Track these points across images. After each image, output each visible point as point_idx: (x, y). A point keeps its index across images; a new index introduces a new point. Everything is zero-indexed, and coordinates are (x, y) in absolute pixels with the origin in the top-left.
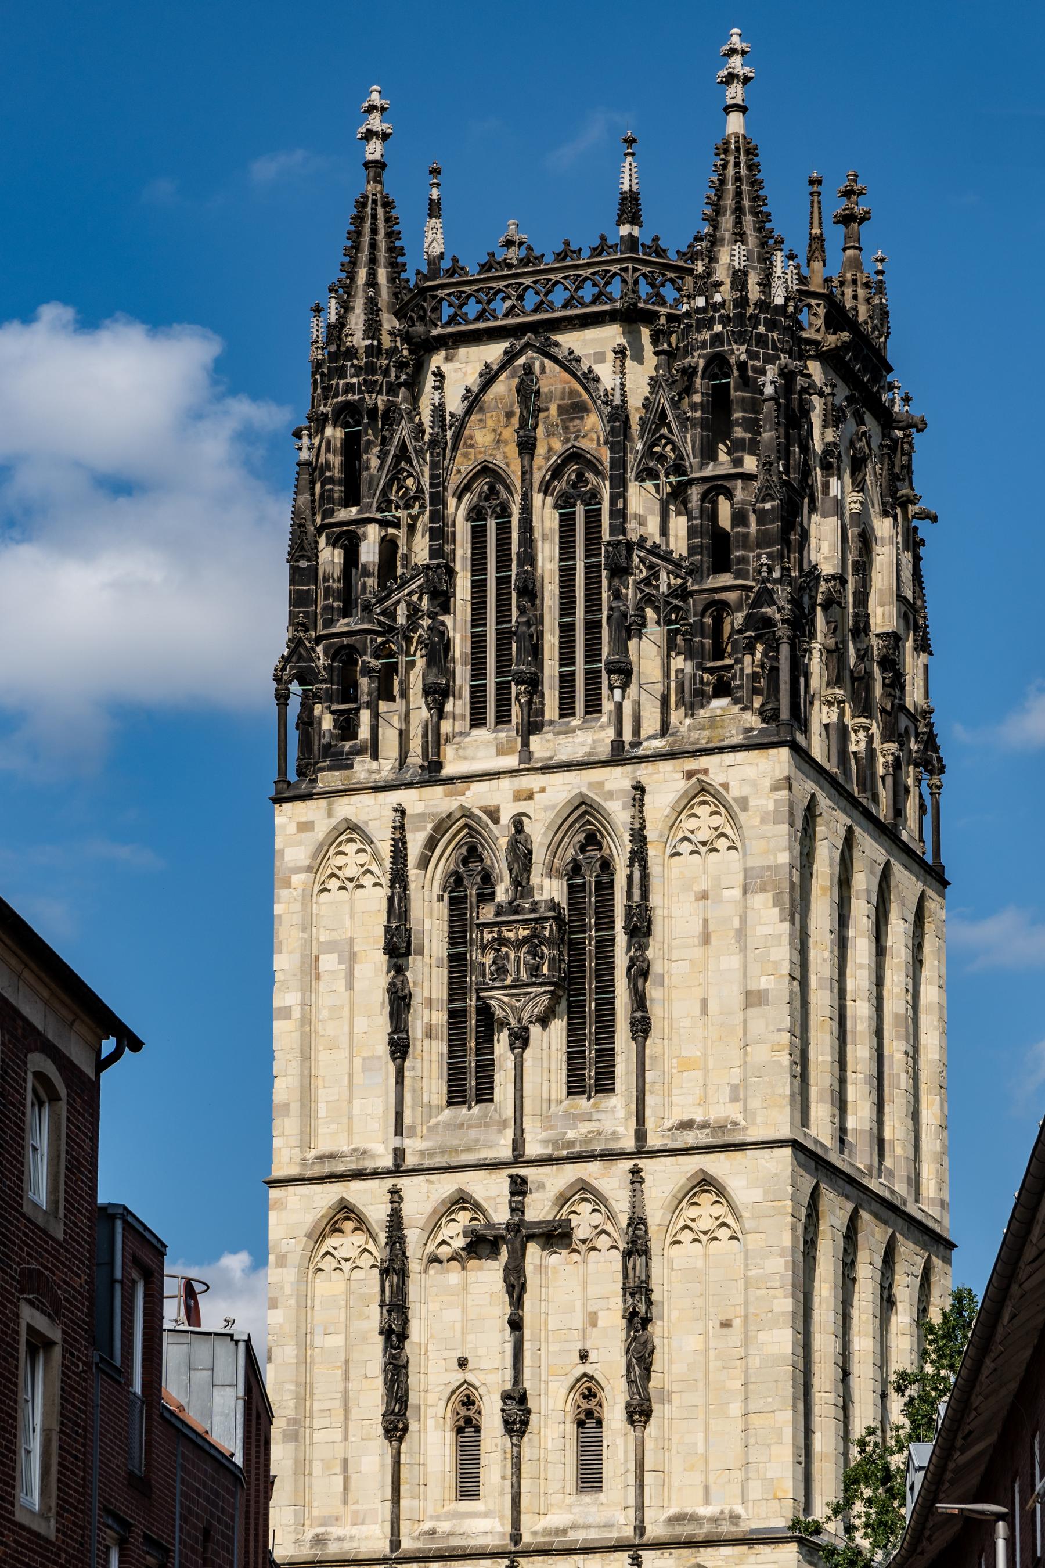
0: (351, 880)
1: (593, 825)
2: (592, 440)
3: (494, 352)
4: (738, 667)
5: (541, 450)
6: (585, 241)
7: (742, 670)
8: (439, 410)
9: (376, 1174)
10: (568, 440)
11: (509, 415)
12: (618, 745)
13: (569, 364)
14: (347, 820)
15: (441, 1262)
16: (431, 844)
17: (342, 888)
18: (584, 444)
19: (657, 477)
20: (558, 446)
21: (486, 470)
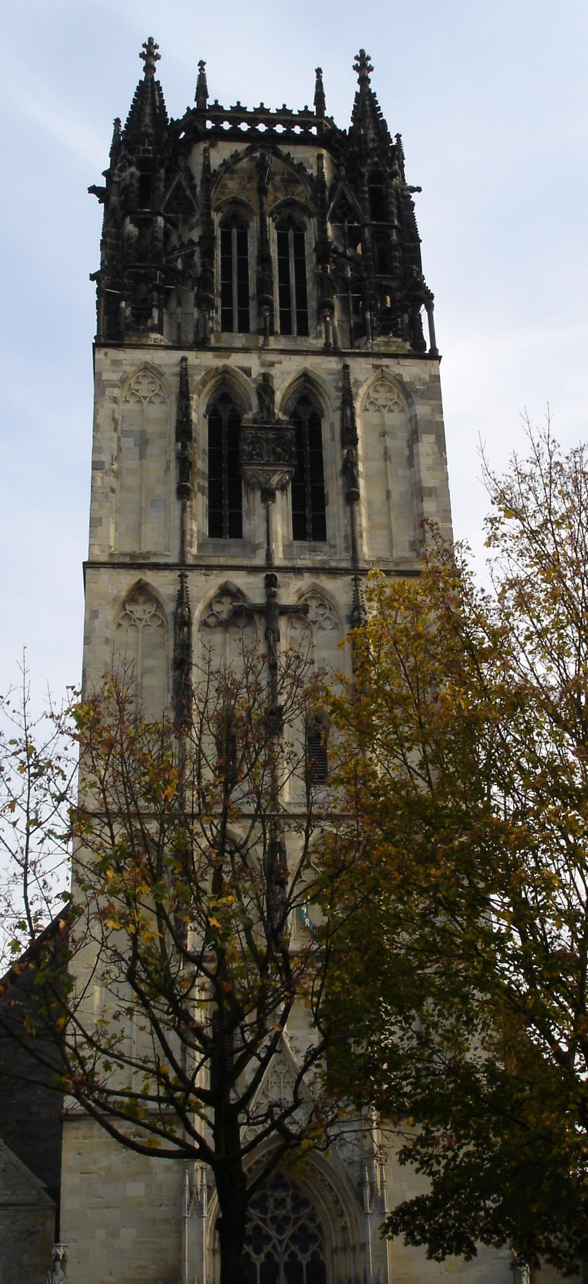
0: (145, 398)
1: (309, 389)
2: (302, 197)
3: (241, 147)
4: (399, 320)
5: (271, 197)
6: (296, 108)
7: (402, 321)
8: (206, 167)
9: (167, 567)
10: (287, 195)
11: (250, 178)
12: (327, 344)
13: (287, 159)
14: (147, 362)
15: (210, 627)
16: (204, 383)
17: (139, 402)
18: (297, 198)
19: (343, 222)
20: (281, 197)
21: (235, 202)
